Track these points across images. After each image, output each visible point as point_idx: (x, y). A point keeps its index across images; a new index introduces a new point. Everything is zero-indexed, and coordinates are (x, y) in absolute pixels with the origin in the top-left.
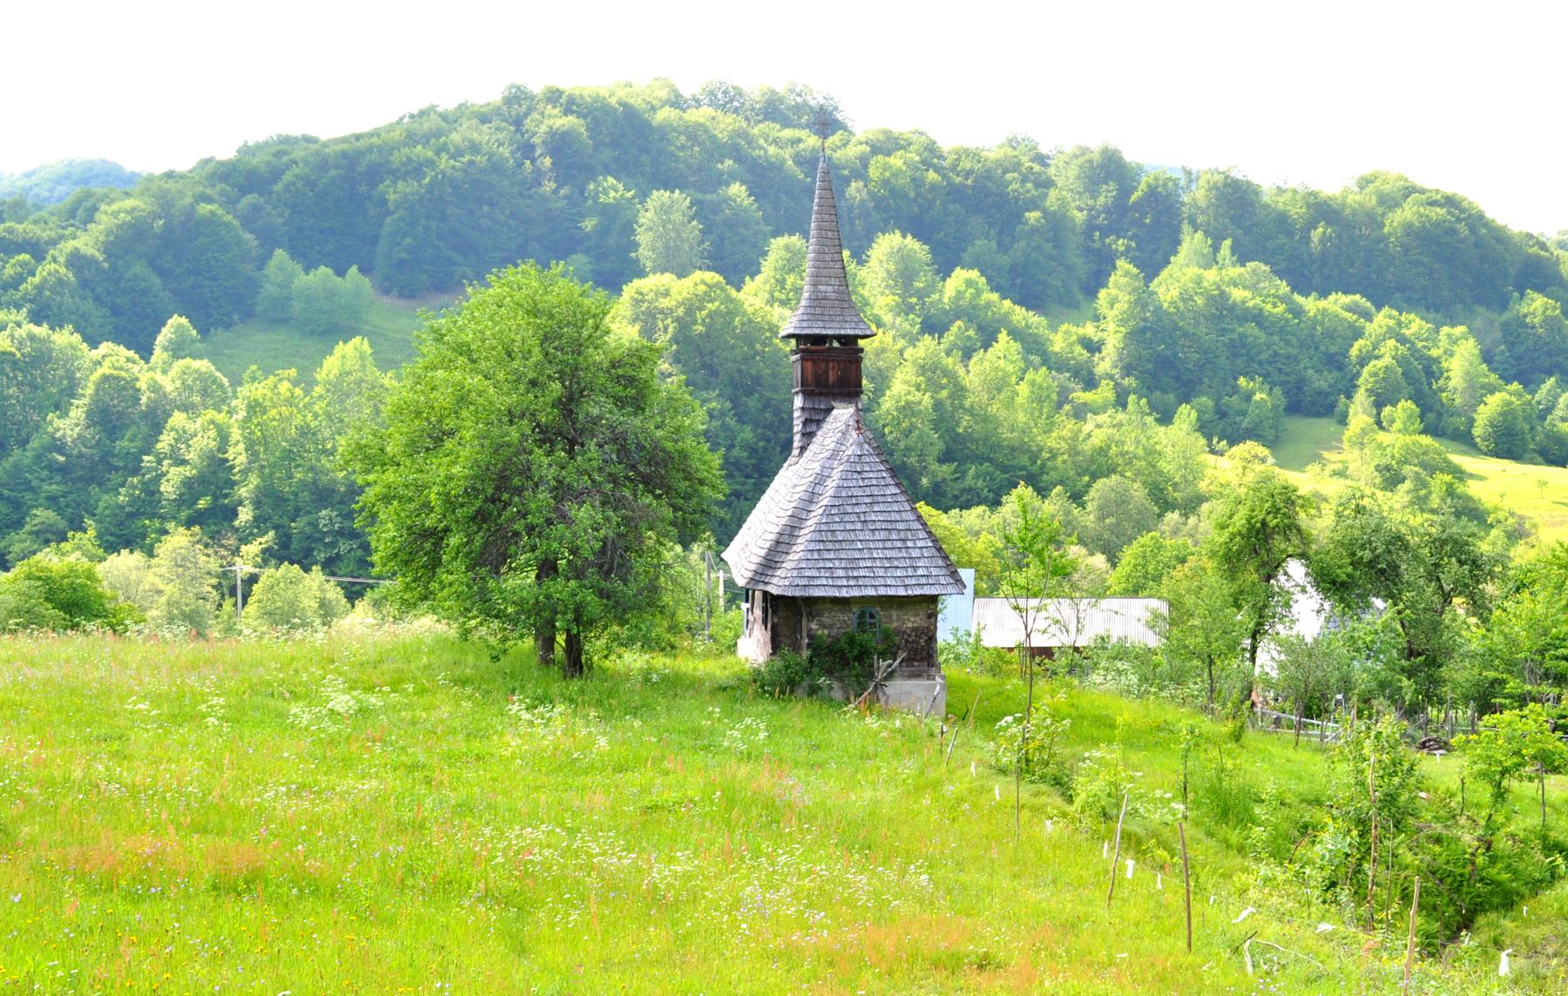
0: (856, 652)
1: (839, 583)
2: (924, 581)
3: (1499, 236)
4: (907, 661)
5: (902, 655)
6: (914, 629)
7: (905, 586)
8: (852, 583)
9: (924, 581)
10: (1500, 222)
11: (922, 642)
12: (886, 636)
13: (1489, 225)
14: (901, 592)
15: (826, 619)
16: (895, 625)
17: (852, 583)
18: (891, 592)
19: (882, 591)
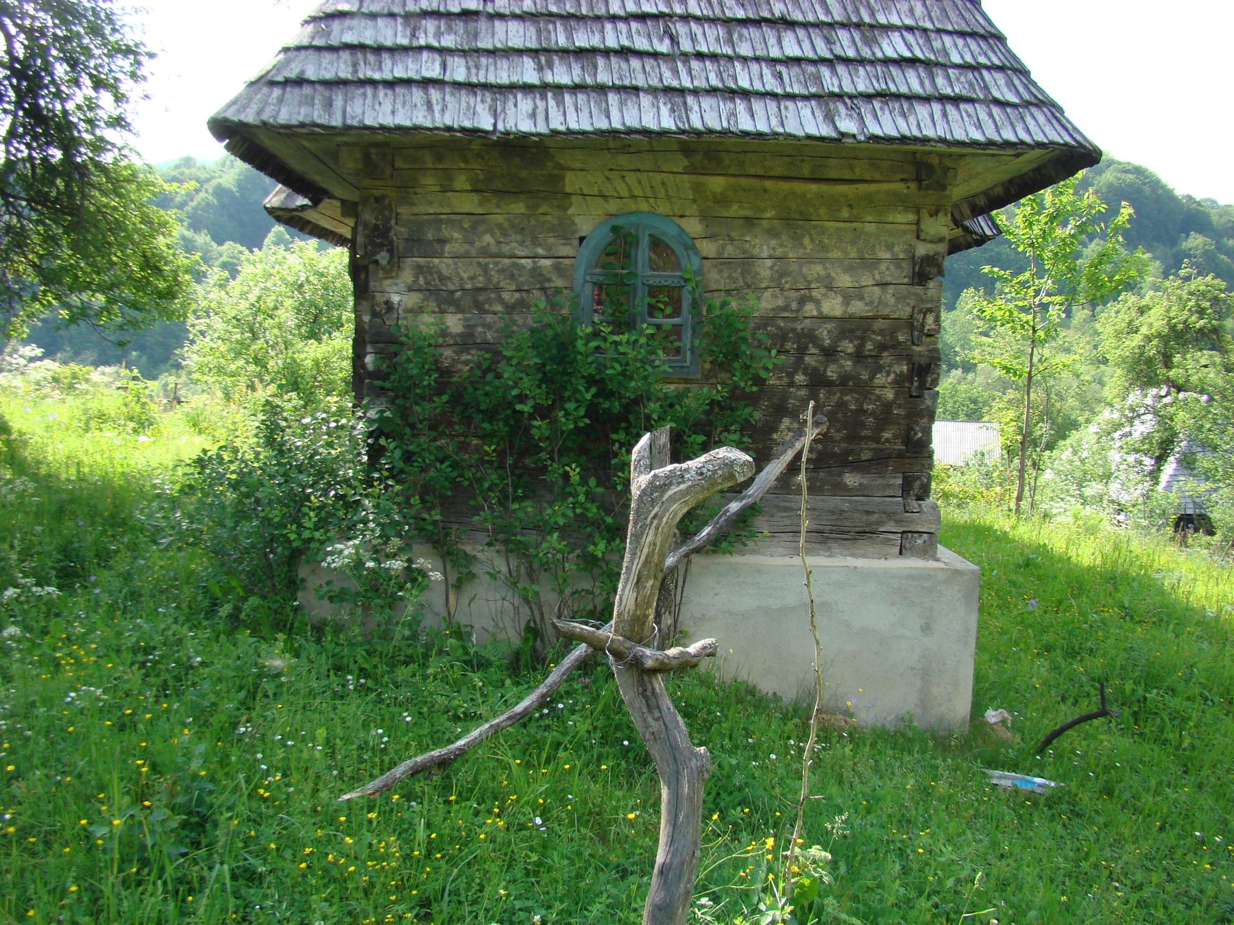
0: (571, 416)
1: (502, 73)
2: (912, 81)
3: (1169, 195)
4: (827, 462)
5: (803, 437)
6: (851, 327)
7: (825, 99)
8: (561, 74)
9: (912, 81)
10: (1170, 187)
11: (885, 386)
12: (727, 346)
13: (1163, 187)
14: (806, 121)
15: (452, 266)
16: (766, 303)
17: (561, 74)
18: (755, 119)
19: (707, 115)
